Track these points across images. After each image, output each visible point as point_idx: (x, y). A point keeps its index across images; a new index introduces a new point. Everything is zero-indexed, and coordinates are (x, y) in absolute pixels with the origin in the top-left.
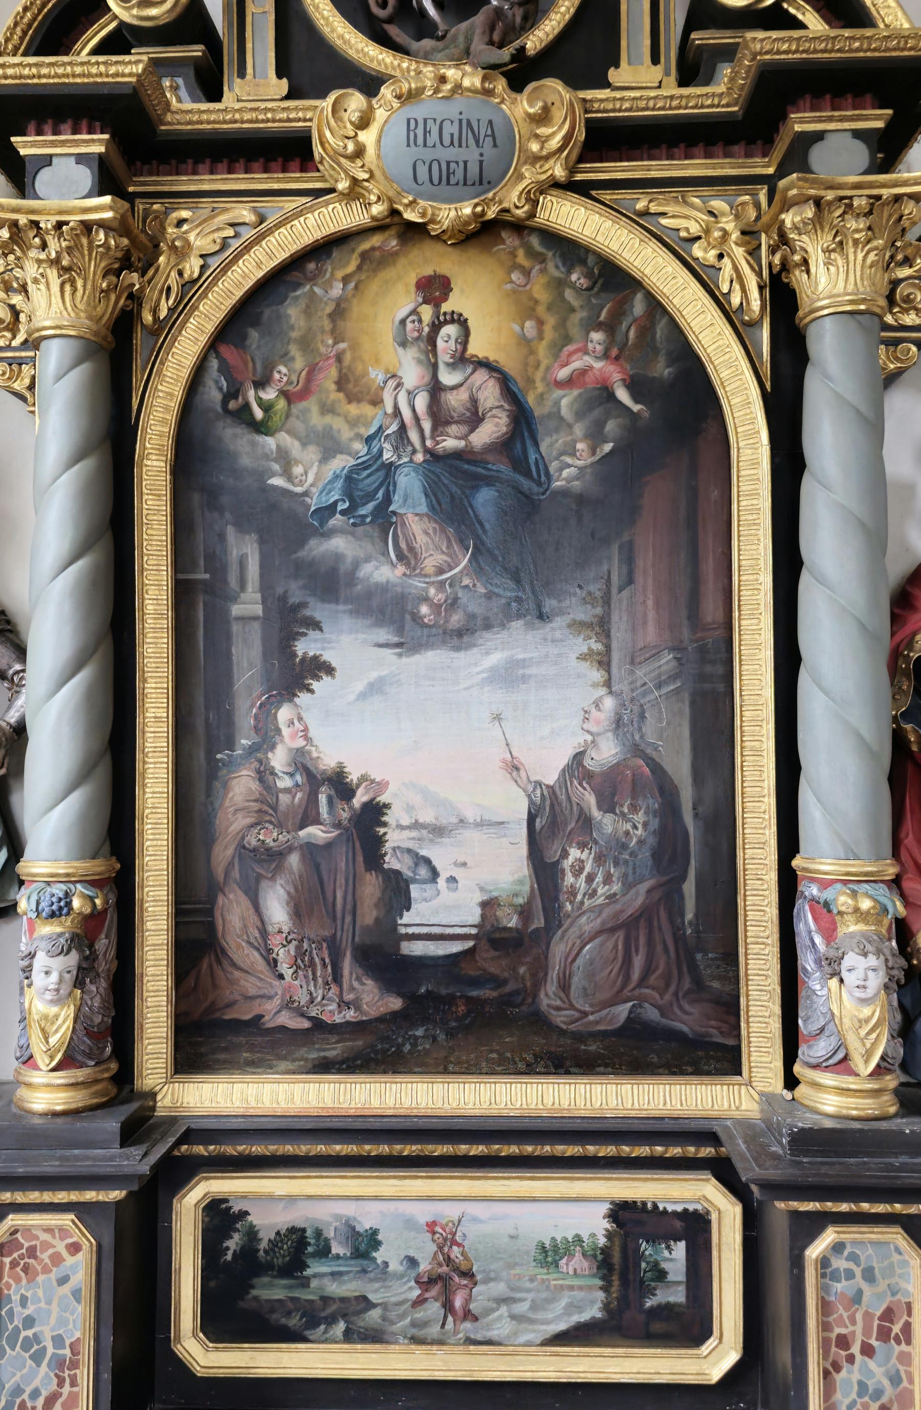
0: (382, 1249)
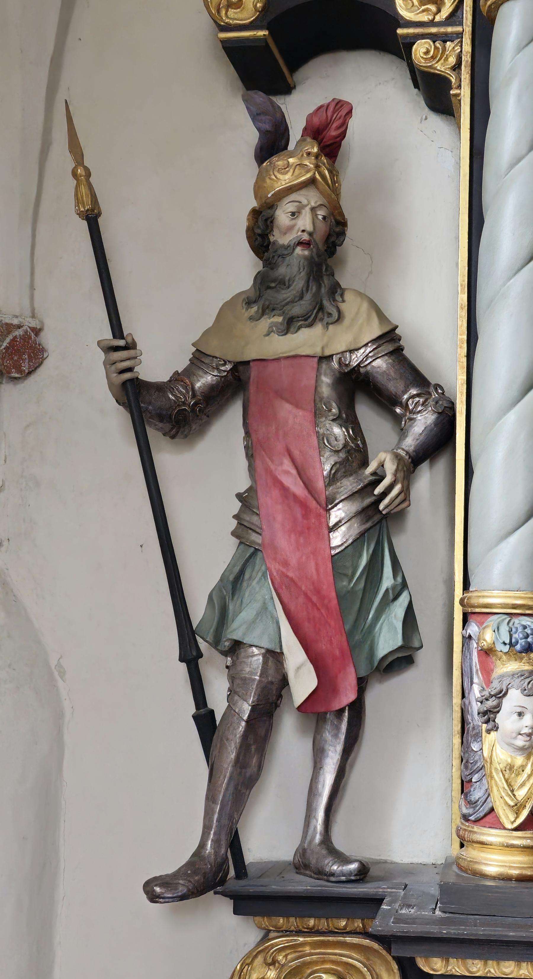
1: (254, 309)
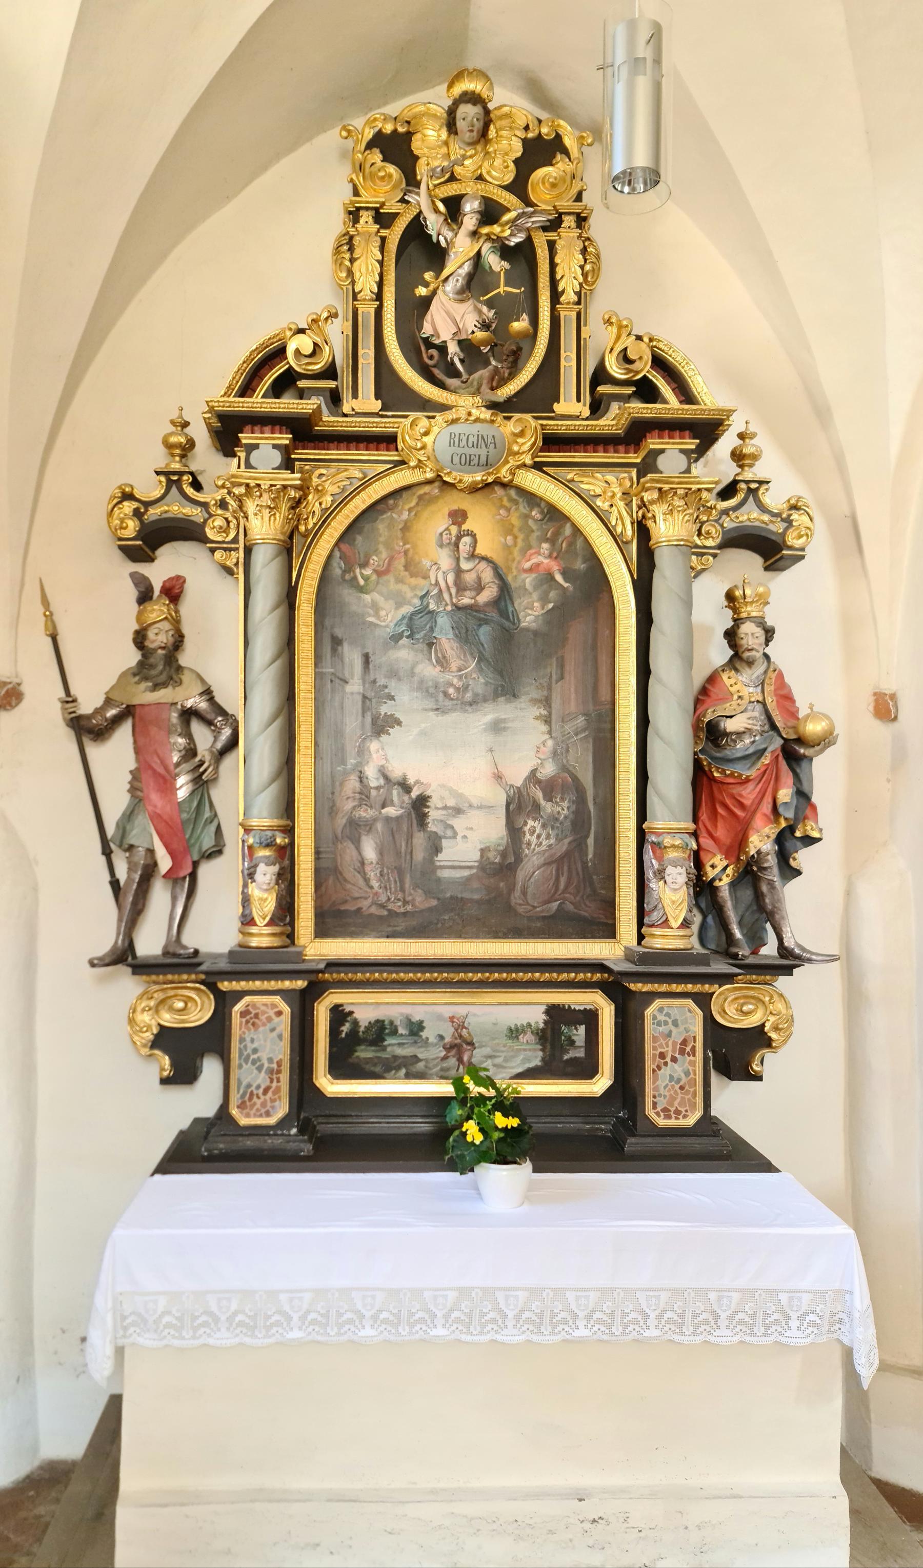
0: (425, 1031)
1: (137, 678)
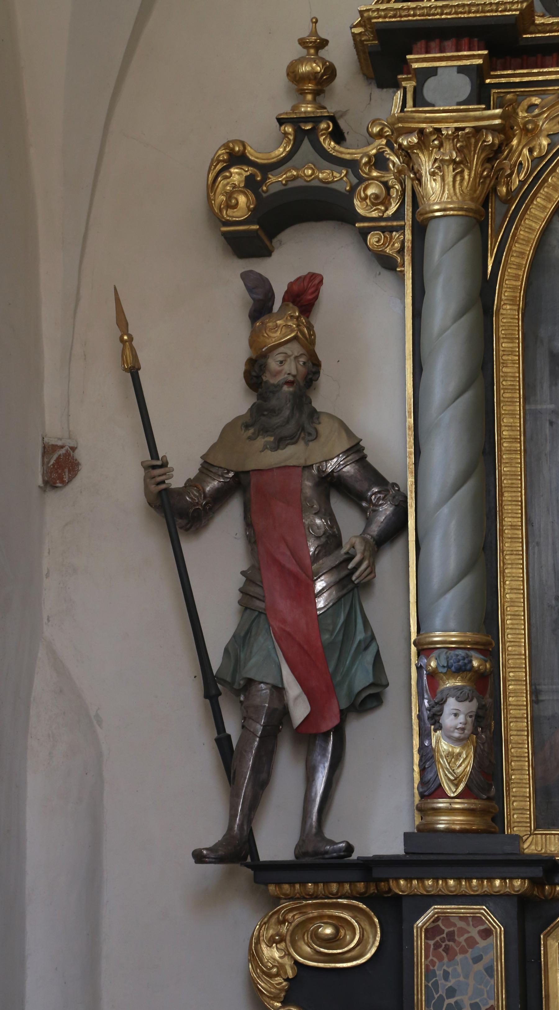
1: (252, 431)
